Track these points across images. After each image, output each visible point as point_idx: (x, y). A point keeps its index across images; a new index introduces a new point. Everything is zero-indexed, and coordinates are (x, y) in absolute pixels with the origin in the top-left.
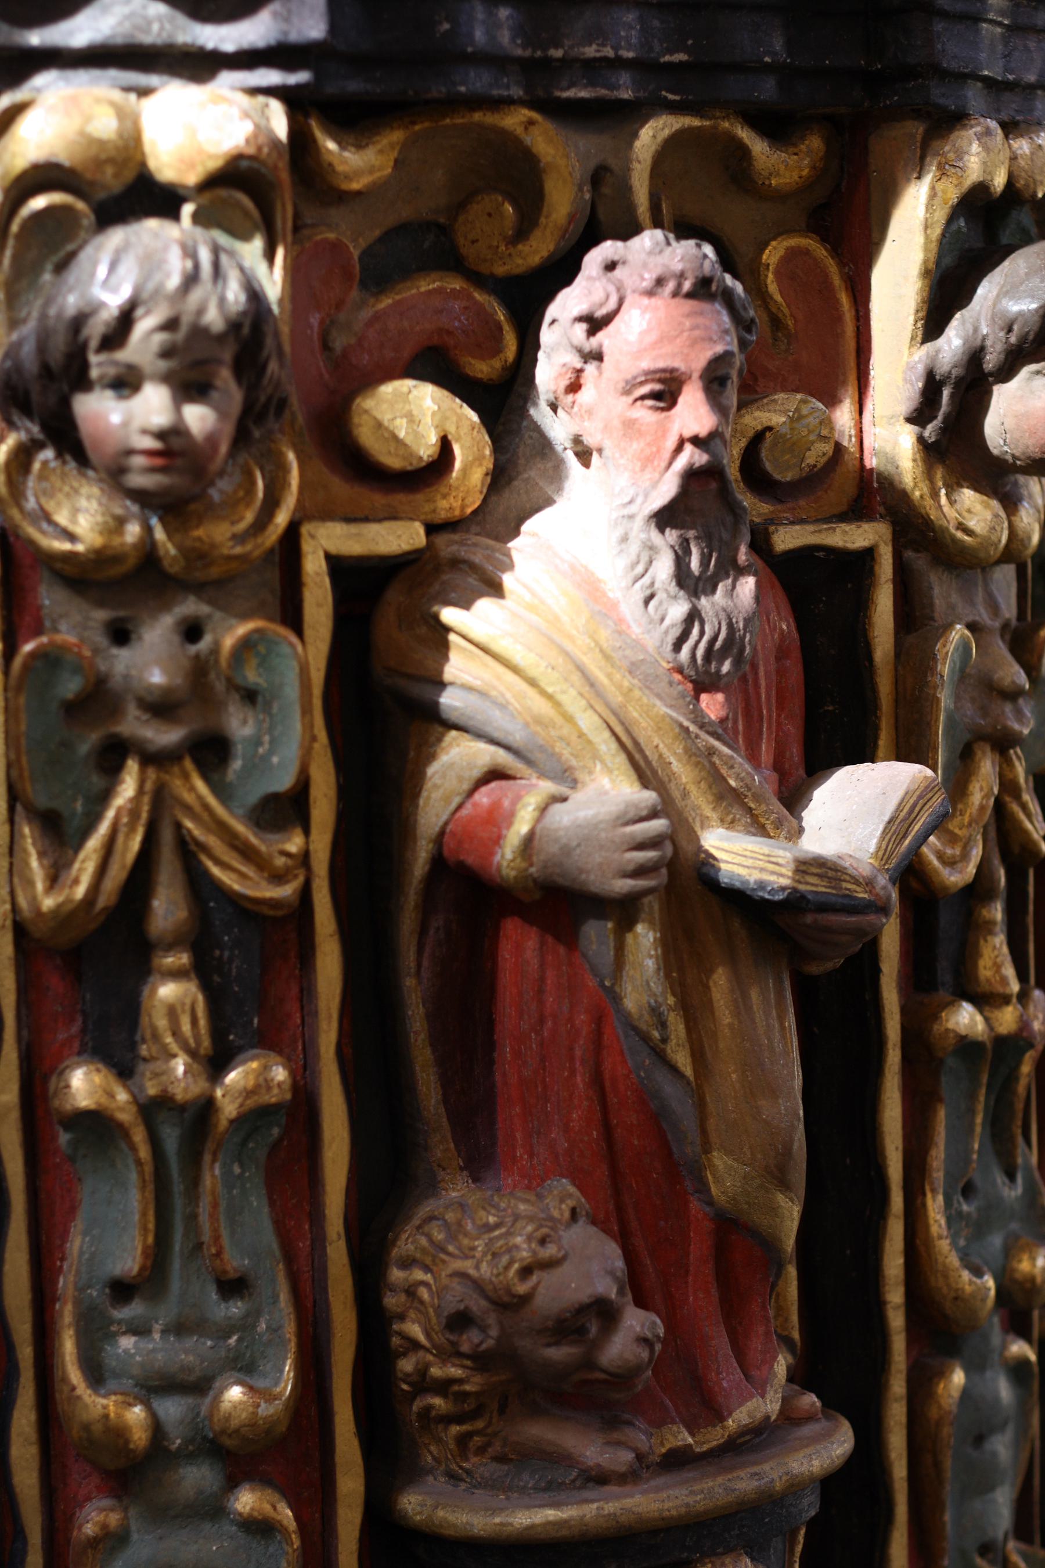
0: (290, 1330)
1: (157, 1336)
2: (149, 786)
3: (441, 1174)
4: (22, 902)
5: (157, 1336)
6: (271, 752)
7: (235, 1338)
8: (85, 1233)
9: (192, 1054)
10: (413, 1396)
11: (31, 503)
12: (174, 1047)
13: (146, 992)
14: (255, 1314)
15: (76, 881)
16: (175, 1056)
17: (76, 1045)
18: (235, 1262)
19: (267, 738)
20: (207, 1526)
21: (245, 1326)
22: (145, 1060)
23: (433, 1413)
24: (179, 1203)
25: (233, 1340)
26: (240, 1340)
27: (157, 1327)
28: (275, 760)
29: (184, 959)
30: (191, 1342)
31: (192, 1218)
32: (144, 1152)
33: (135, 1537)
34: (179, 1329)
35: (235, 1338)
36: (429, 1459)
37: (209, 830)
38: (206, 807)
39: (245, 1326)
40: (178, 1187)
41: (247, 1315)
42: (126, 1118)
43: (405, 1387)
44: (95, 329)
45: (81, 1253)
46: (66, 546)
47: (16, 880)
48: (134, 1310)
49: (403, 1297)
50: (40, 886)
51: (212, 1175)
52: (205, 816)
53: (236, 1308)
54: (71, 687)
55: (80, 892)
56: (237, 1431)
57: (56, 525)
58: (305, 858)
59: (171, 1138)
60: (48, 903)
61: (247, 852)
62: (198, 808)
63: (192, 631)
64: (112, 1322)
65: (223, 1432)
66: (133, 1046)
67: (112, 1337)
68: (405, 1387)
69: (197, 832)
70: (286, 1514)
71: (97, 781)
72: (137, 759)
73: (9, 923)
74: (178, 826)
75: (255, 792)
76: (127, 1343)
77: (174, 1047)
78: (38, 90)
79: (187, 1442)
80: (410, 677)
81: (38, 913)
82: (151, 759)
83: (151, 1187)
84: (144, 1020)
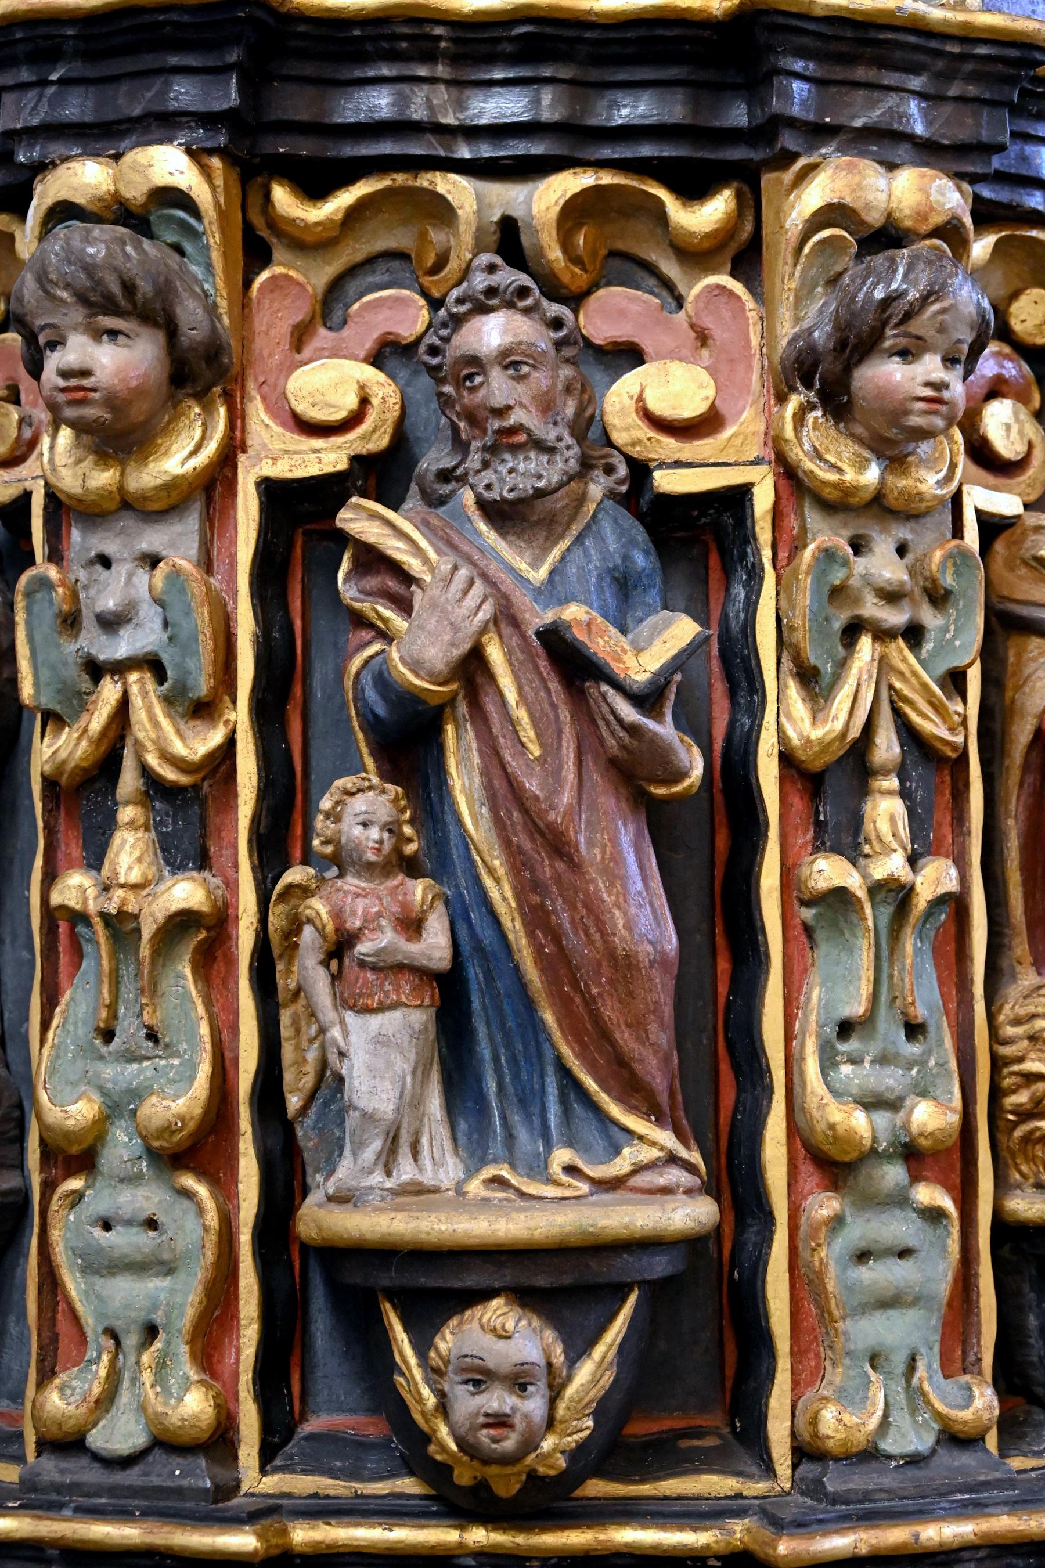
0: (953, 1065)
1: (867, 1065)
2: (877, 656)
3: (1019, 968)
4: (791, 733)
5: (867, 1065)
6: (955, 637)
7: (915, 1070)
8: (822, 985)
9: (905, 849)
10: (1015, 1125)
11: (807, 447)
12: (895, 845)
13: (868, 807)
14: (928, 1053)
15: (836, 718)
16: (895, 851)
17: (810, 848)
18: (920, 1012)
19: (952, 627)
20: (897, 1212)
21: (922, 1063)
22: (867, 856)
23: (1038, 1134)
24: (885, 965)
25: (914, 1072)
26: (918, 1072)
27: (868, 1059)
28: (957, 643)
29: (893, 783)
30: (890, 1070)
31: (891, 977)
32: (870, 923)
33: (849, 1220)
34: (883, 1060)
35: (915, 1070)
36: (1018, 1176)
37: (914, 690)
38: (915, 673)
39: (922, 1063)
40: (885, 953)
41: (923, 1053)
42: (861, 894)
43: (1011, 1117)
44: (899, 309)
45: (820, 1000)
46: (832, 477)
47: (783, 719)
48: (852, 1045)
49: (1026, 1043)
50: (807, 722)
51: (909, 943)
52: (914, 680)
53: (913, 1050)
54: (837, 577)
55: (839, 725)
56: (931, 1134)
57: (827, 461)
58: (964, 723)
59: (887, 912)
60: (816, 734)
61: (938, 708)
62: (908, 674)
63: (902, 550)
64: (837, 1053)
65: (921, 1134)
66: (857, 846)
67: (835, 1065)
68: (1011, 1117)
69: (907, 692)
70: (947, 1203)
71: (841, 651)
72: (869, 635)
73: (776, 751)
74: (891, 687)
75: (943, 666)
76: (846, 1069)
77: (895, 845)
78: (824, 157)
79: (891, 1144)
80: (1017, 602)
81: (808, 740)
82: (882, 635)
83: (873, 949)
84: (868, 827)
